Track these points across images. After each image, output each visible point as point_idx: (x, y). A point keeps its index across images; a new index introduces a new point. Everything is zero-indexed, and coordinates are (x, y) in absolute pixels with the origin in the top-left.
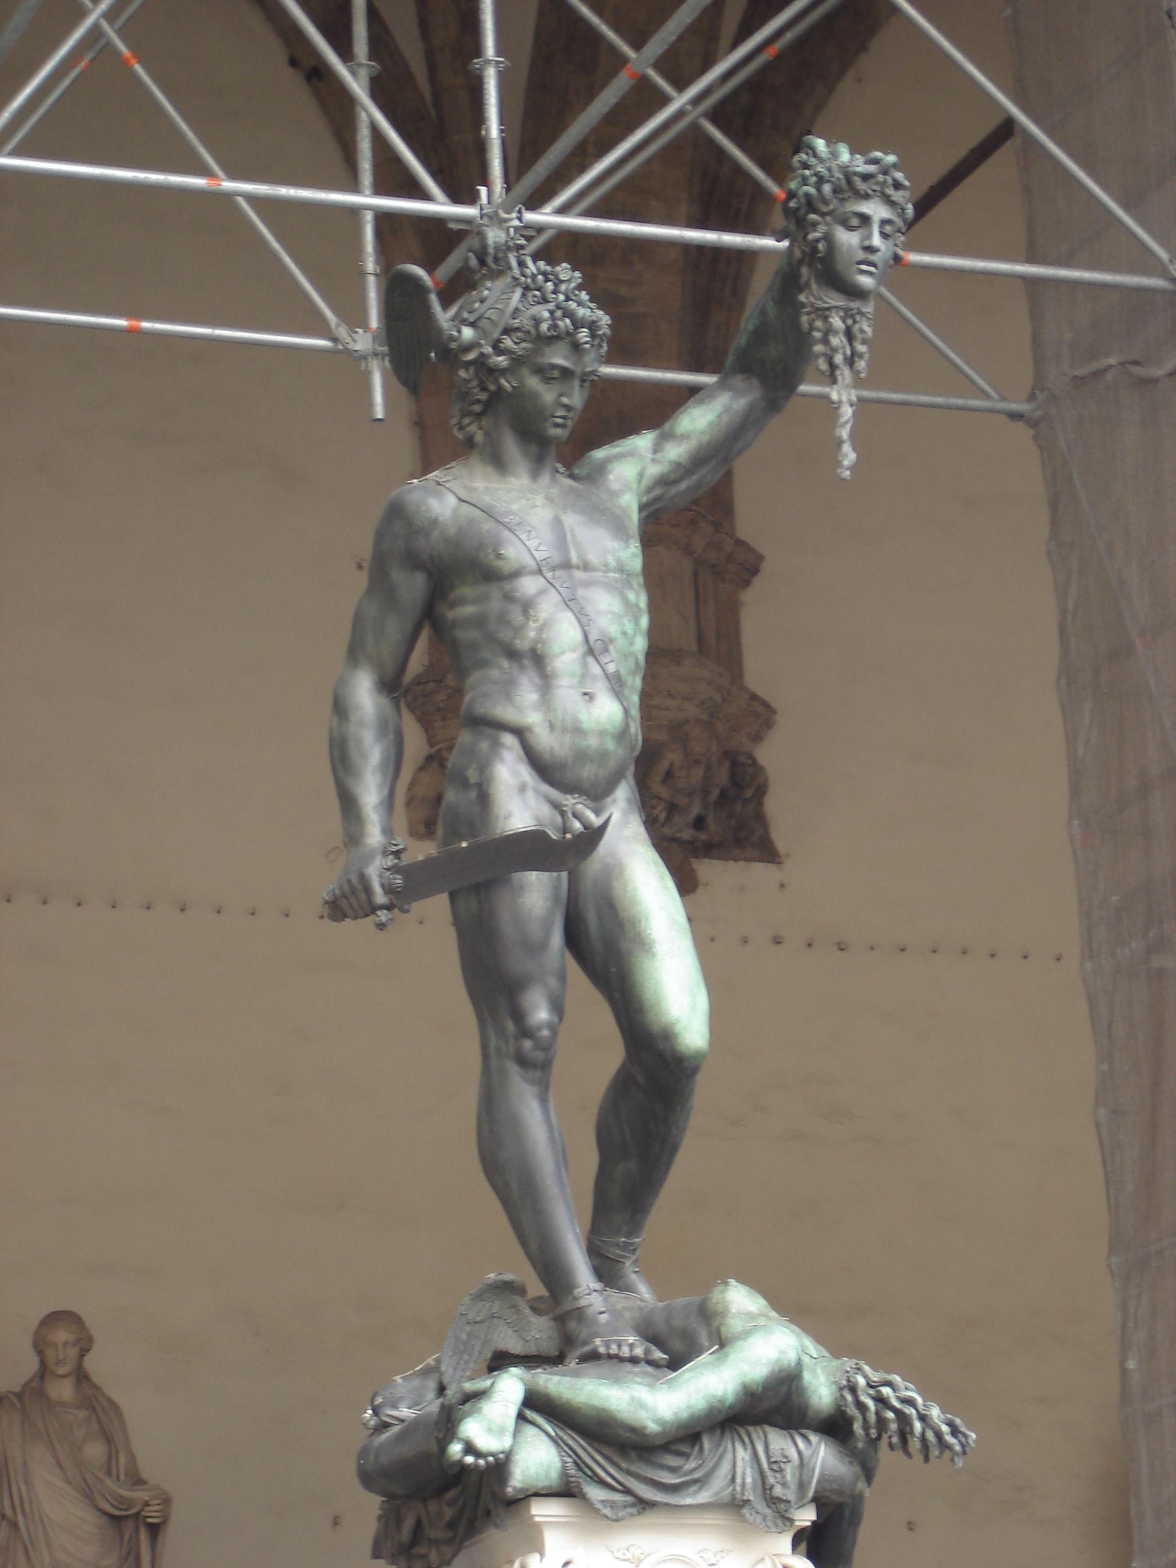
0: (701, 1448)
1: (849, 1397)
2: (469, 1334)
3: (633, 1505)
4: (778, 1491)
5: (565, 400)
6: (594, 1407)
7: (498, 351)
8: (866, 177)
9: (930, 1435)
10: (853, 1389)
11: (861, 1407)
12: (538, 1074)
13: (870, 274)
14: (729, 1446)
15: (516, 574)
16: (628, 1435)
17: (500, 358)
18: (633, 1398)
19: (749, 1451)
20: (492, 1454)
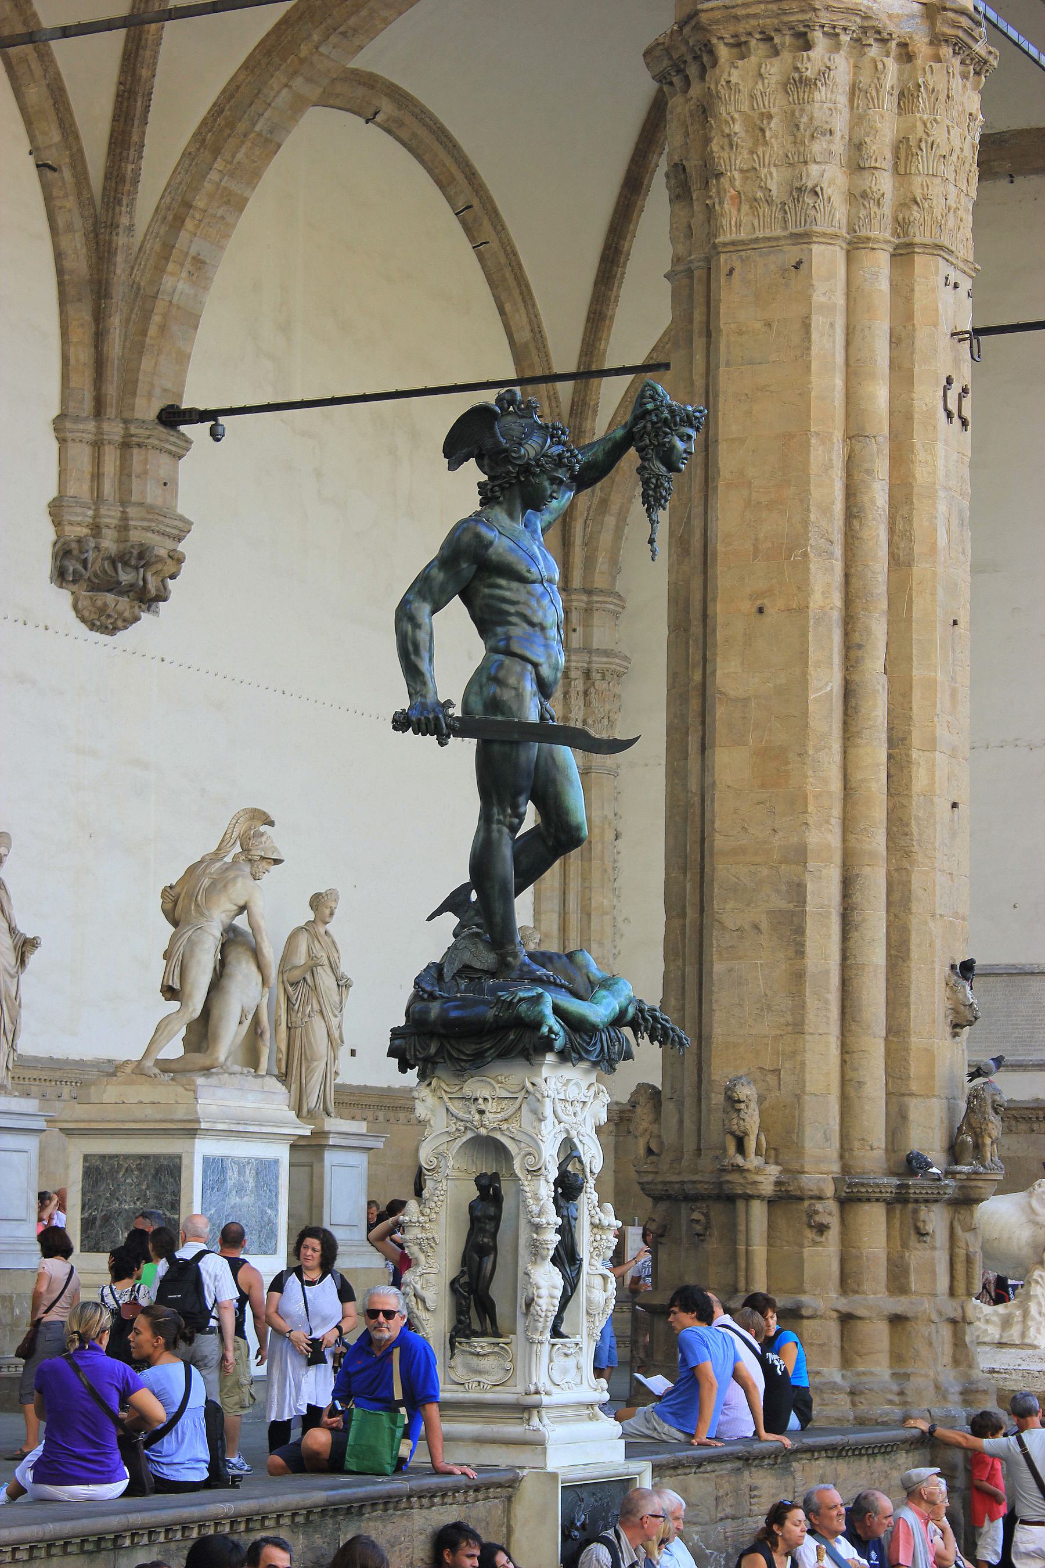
7: (538, 466)
8: (696, 418)
10: (641, 1011)
13: (683, 463)
15: (534, 582)
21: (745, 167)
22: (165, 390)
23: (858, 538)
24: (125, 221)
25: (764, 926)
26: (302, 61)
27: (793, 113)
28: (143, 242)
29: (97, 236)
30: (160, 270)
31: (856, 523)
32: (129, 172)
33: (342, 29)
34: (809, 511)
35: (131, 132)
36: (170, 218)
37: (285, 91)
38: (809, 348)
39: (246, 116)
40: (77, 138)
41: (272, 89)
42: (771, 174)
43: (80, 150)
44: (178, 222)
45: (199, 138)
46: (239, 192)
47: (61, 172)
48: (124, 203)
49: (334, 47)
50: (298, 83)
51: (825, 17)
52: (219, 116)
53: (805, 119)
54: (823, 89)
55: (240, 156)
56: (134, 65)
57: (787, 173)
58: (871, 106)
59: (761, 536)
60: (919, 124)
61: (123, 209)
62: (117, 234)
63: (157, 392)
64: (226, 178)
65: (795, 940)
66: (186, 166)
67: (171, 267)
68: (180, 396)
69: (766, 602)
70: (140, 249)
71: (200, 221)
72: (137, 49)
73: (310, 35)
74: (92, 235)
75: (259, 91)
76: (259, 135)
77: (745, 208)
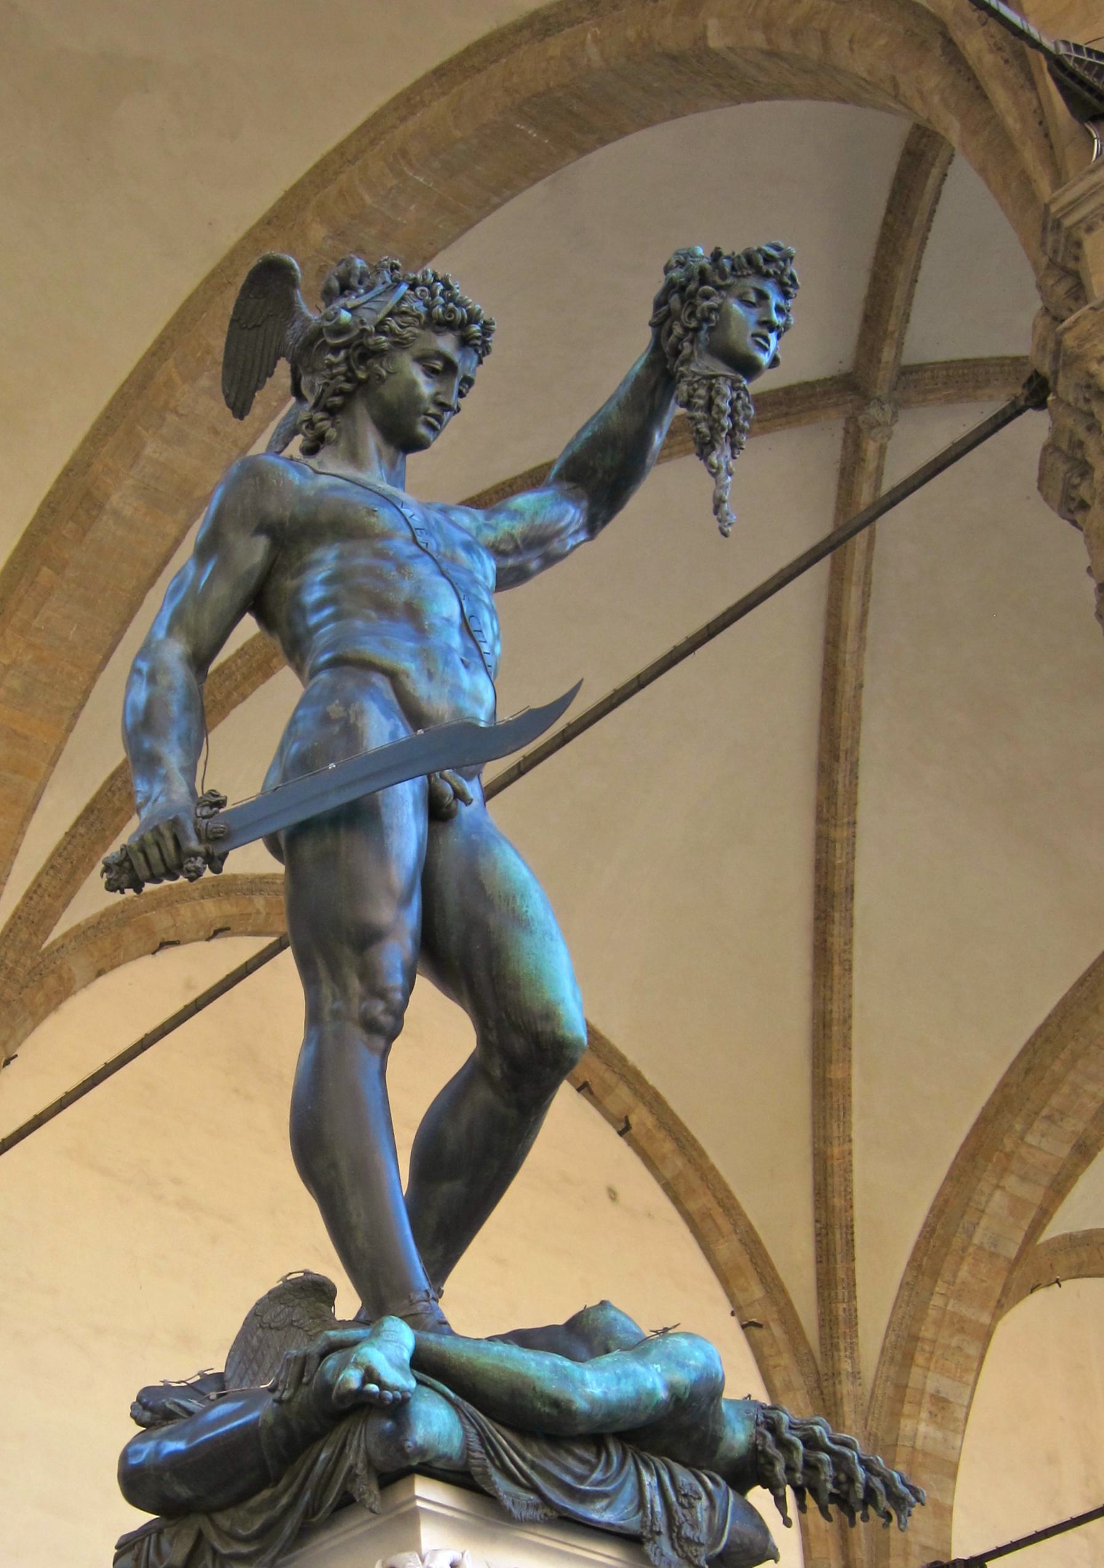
0: (608, 1463)
1: (769, 1436)
2: (260, 1341)
3: (536, 1507)
4: (687, 1531)
5: (441, 398)
6: (504, 1370)
9: (877, 1482)
11: (785, 1446)
12: (380, 1042)
14: (633, 1468)
16: (547, 1410)
17: (384, 338)
18: (555, 1365)
19: (655, 1479)
20: (397, 1389)
22: (925, 1548)
24: (846, 1366)
26: (1009, 1156)
28: (873, 1392)
29: (822, 1393)
30: (896, 1415)
32: (841, 1313)
33: (1045, 1112)
35: (835, 1269)
36: (898, 1357)
37: (998, 1194)
39: (960, 1230)
40: (783, 1291)
41: (982, 1193)
43: (789, 1303)
44: (908, 1360)
45: (915, 1264)
46: (973, 1317)
47: (768, 1327)
48: (842, 1346)
49: (1043, 1136)
50: (1011, 1181)
52: (931, 1236)
55: (964, 1273)
56: (826, 1197)
61: (842, 1354)
62: (840, 1382)
63: (915, 1549)
64: (952, 1302)
66: (906, 1298)
67: (907, 1408)
68: (949, 1554)
70: (872, 1397)
71: (932, 1353)
72: (825, 1179)
73: (1011, 1127)
74: (817, 1393)
75: (970, 1199)
76: (980, 1248)
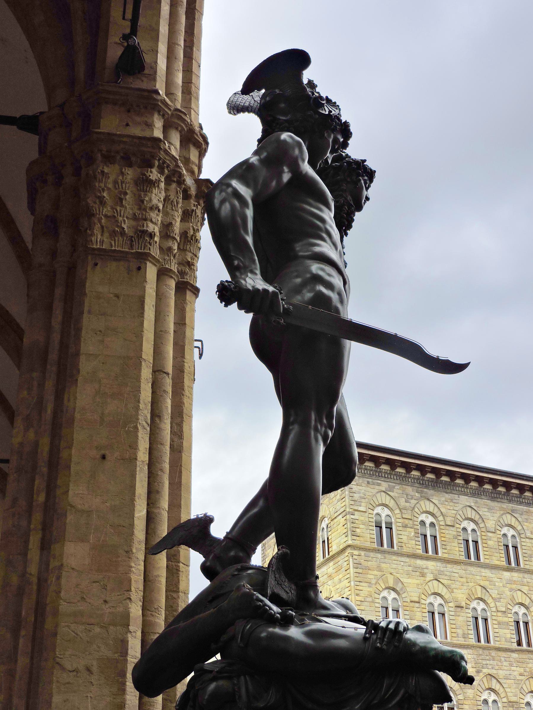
21: (109, 214)
23: (158, 428)
25: (95, 669)
27: (140, 196)
31: (157, 419)
34: (139, 402)
38: (143, 313)
42: (124, 221)
51: (162, 155)
53: (147, 199)
54: (157, 188)
57: (133, 223)
58: (174, 208)
59: (107, 411)
60: (191, 228)
65: (118, 681)
69: (107, 453)
77: (106, 234)
